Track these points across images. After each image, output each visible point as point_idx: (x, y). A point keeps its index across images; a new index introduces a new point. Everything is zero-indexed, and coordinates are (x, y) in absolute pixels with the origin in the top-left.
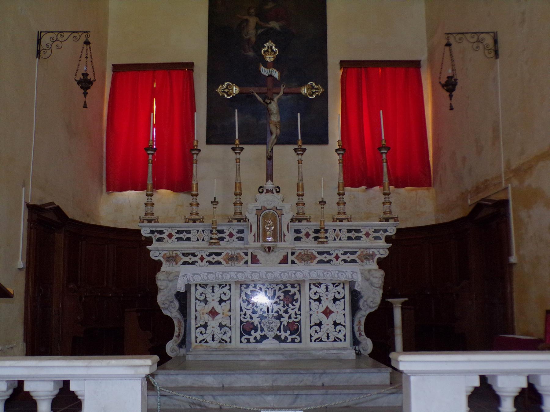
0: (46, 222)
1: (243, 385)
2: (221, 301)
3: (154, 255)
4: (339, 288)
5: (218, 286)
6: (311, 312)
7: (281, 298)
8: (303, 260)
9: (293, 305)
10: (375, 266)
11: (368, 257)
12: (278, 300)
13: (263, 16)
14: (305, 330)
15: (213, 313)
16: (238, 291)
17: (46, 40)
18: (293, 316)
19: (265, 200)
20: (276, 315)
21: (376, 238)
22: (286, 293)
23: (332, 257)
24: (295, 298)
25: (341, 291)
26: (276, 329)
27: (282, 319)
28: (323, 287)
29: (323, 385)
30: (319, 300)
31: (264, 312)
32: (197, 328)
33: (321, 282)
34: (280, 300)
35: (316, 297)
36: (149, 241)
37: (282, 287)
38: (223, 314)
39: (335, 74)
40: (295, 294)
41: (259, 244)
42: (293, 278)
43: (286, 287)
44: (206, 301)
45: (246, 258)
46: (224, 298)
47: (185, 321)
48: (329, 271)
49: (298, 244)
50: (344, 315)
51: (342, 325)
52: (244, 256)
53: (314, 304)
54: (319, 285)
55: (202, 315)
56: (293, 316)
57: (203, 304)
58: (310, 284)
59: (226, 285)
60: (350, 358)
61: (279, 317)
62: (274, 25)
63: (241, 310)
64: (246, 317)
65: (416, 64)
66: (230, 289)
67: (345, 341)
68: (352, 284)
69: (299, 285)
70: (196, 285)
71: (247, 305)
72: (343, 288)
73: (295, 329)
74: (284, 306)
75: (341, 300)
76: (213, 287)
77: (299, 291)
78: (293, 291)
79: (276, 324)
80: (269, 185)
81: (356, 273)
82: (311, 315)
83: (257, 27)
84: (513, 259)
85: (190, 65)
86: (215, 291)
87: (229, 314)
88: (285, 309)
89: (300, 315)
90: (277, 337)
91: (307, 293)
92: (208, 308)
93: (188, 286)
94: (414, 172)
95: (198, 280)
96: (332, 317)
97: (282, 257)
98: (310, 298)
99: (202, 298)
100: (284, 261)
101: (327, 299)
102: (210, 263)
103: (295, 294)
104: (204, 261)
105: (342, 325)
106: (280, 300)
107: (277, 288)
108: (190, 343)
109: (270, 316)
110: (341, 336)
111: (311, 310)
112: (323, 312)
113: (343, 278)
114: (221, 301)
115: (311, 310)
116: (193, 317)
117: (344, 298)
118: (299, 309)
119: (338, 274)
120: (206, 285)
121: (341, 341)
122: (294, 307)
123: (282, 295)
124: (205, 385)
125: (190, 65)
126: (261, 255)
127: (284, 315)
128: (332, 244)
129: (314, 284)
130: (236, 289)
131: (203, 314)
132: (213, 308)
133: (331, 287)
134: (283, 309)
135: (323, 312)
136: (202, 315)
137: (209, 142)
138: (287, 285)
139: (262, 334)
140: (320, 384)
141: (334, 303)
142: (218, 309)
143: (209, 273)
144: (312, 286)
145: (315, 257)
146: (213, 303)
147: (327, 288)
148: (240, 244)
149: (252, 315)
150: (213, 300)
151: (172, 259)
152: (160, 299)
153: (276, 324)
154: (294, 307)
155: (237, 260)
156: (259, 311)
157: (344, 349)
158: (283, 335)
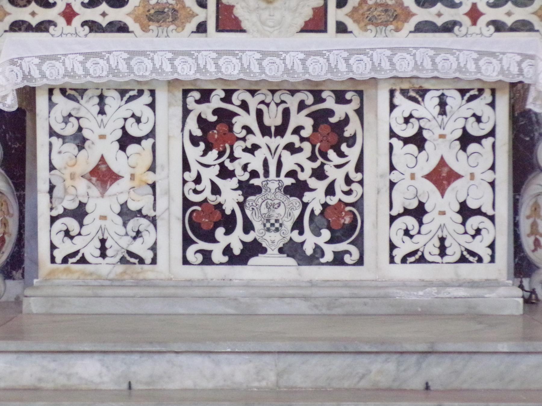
1: (189, 384)
2: (126, 141)
4: (480, 106)
5: (117, 95)
6: (395, 176)
7: (305, 133)
8: (372, 21)
9: (341, 155)
12: (295, 139)
14: (376, 230)
15: (103, 175)
16: (178, 111)
18: (340, 186)
20: (289, 181)
22: (320, 117)
23: (459, 14)
24: (347, 134)
25: (486, 112)
26: (289, 224)
27: (307, 197)
28: (431, 101)
29: (427, 387)
30: (418, 140)
31: (254, 174)
32: (53, 220)
33: (426, 86)
34: (302, 139)
35: (410, 131)
37: (309, 99)
38: (133, 177)
40: (346, 121)
42: (342, 73)
43: (318, 97)
44: (80, 140)
45: (201, 15)
46: (134, 130)
47: (21, 201)
48: (450, 51)
50: (492, 184)
51: (485, 215)
52: (197, 9)
53: (404, 154)
55: (69, 182)
56: (340, 186)
57: (71, 148)
58: (392, 93)
59: (141, 93)
60: (507, 312)
61: (298, 189)
63: (186, 167)
64: (199, 188)
66: (152, 106)
67: (493, 260)
68: (518, 91)
69: (360, 93)
70: (51, 91)
71: (205, 153)
72: (492, 105)
73: (345, 225)
74: (313, 158)
75: (484, 141)
76: (102, 98)
77: (360, 112)
78: (340, 111)
79: (288, 209)
81: (532, 57)
82: (392, 185)
86: (107, 109)
87: (151, 177)
88: (316, 165)
89: (361, 182)
90: (292, 250)
92: (88, 160)
93: (27, 95)
95: (55, 75)
96: (457, 191)
97: (307, 14)
98: (393, 134)
99: (70, 130)
101: (442, 136)
102: (93, 27)
103: (346, 121)
104: (77, 21)
105: (485, 215)
106: (302, 139)
107: (293, 103)
108: (35, 262)
109: (273, 186)
110: (480, 246)
111: (392, 168)
112: (428, 177)
113: (491, 73)
114: (126, 141)
115: (392, 168)
116: (43, 186)
117: (492, 133)
118: (359, 168)
119: (476, 61)
120: (82, 92)
121: (480, 260)
122: (342, 161)
123: (308, 123)
124: (74, 382)
127: (313, 183)
129: (404, 92)
130: (170, 105)
131: (73, 177)
132: (102, 160)
133: (454, 100)
134: (309, 166)
135: (428, 177)
136: (69, 182)
138: (324, 95)
139: (249, 238)
140: (418, 384)
141: (464, 148)
142: (118, 162)
143: (87, 56)
144: (399, 99)
145: (409, 15)
147: (443, 104)
149: (219, 182)
150: (102, 137)
154: (342, 161)
155: (175, 19)
156: (239, 172)
157: (490, 284)
158: (310, 241)
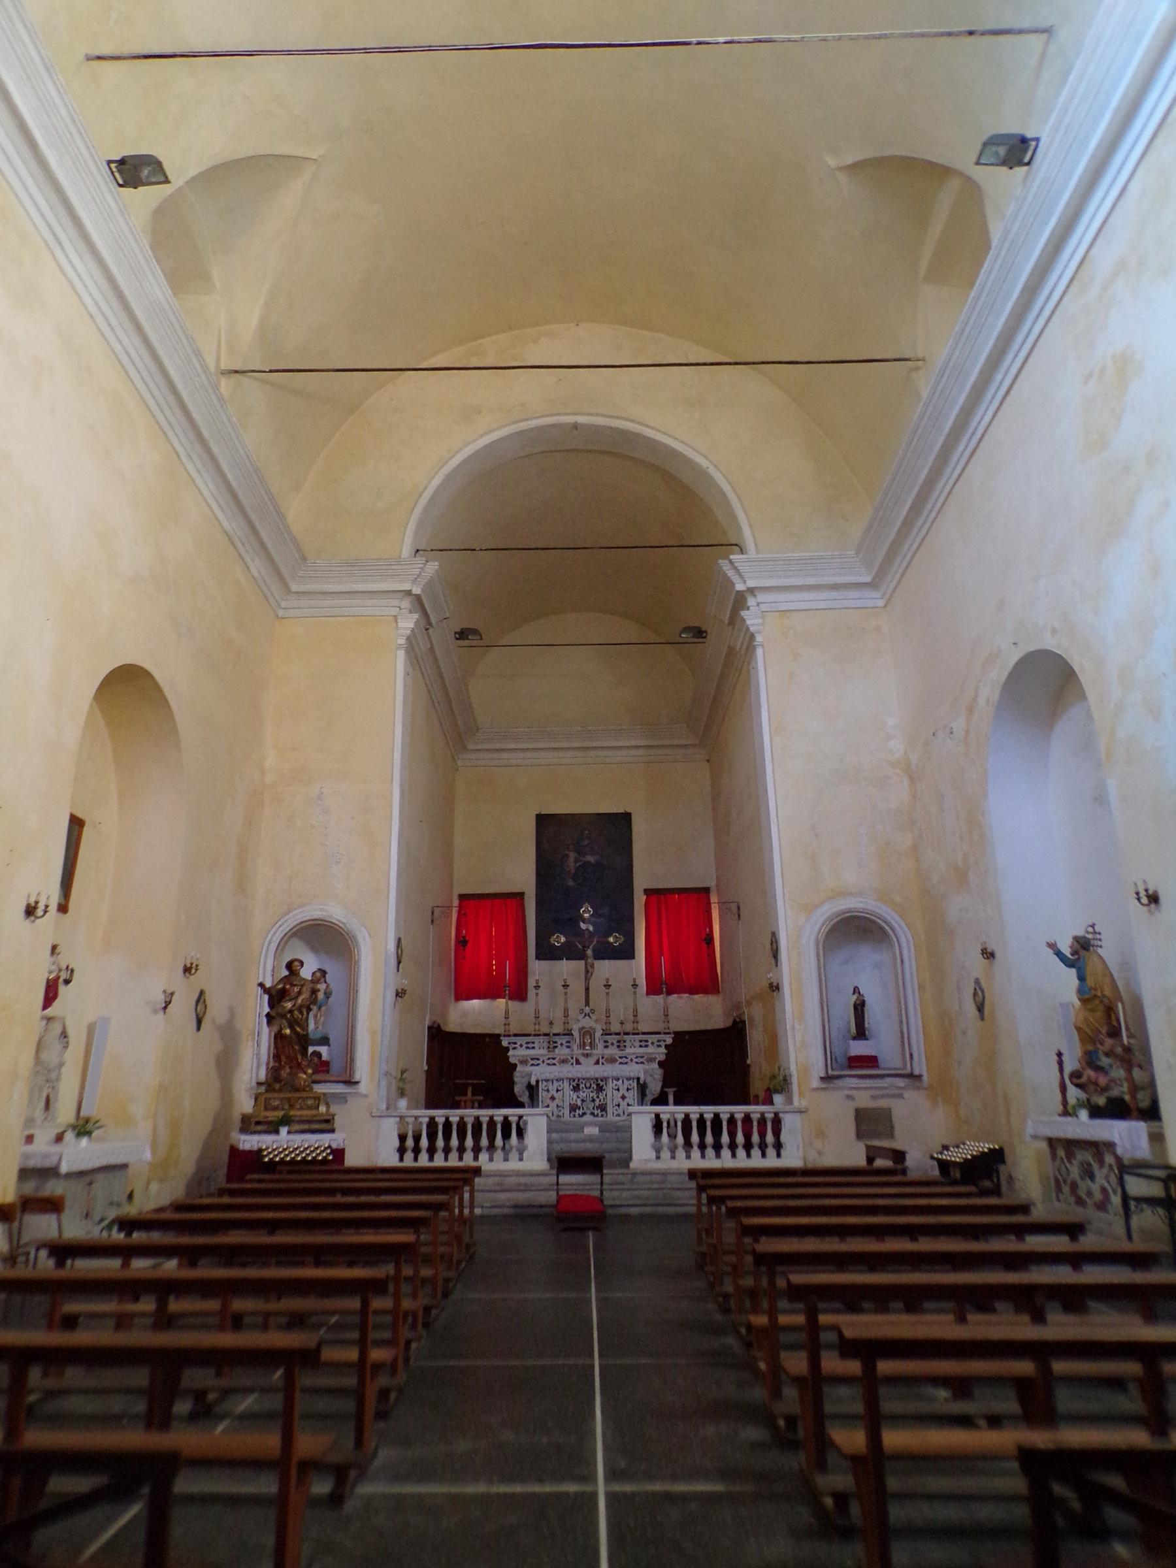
0: (437, 1034)
3: (512, 1060)
10: (656, 1066)
11: (651, 1060)
13: (580, 852)
14: (610, 1109)
15: (553, 1098)
17: (437, 911)
19: (587, 1023)
21: (659, 1046)
36: (507, 1049)
39: (640, 900)
41: (580, 1052)
49: (608, 1052)
54: (618, 1079)
61: (594, 1100)
62: (590, 859)
65: (707, 890)
73: (603, 1108)
79: (591, 1105)
80: (587, 1009)
83: (576, 861)
84: (748, 1062)
85: (522, 894)
90: (592, 1114)
91: (611, 1085)
93: (537, 1082)
94: (705, 982)
95: (544, 1077)
96: (626, 1100)
100: (597, 1063)
113: (632, 1075)
125: (522, 894)
126: (582, 1059)
128: (629, 1051)
137: (539, 957)
142: (556, 1095)
146: (553, 1092)
148: (567, 1051)
151: (524, 1062)
152: (517, 1089)
153: (591, 1105)
